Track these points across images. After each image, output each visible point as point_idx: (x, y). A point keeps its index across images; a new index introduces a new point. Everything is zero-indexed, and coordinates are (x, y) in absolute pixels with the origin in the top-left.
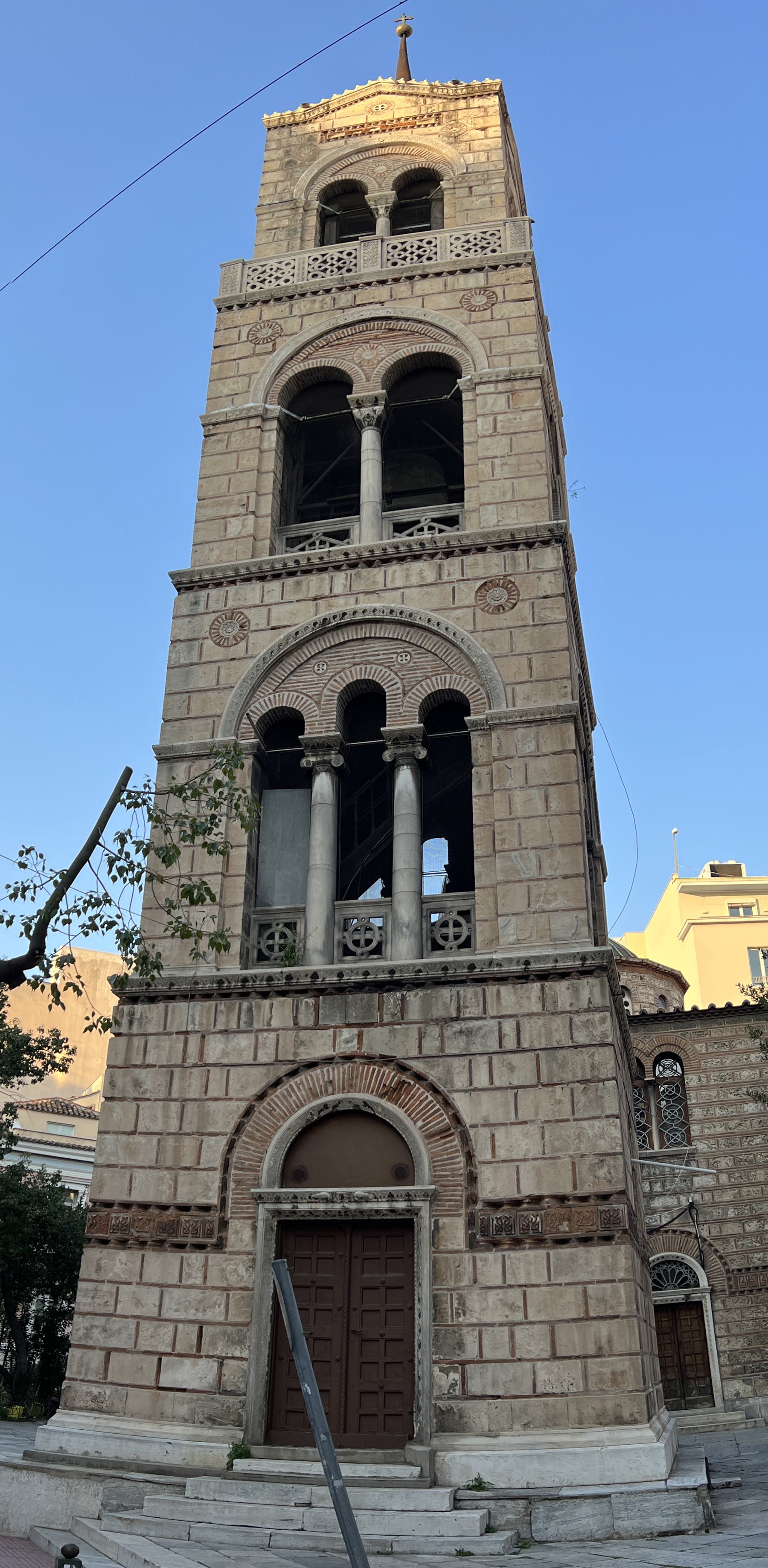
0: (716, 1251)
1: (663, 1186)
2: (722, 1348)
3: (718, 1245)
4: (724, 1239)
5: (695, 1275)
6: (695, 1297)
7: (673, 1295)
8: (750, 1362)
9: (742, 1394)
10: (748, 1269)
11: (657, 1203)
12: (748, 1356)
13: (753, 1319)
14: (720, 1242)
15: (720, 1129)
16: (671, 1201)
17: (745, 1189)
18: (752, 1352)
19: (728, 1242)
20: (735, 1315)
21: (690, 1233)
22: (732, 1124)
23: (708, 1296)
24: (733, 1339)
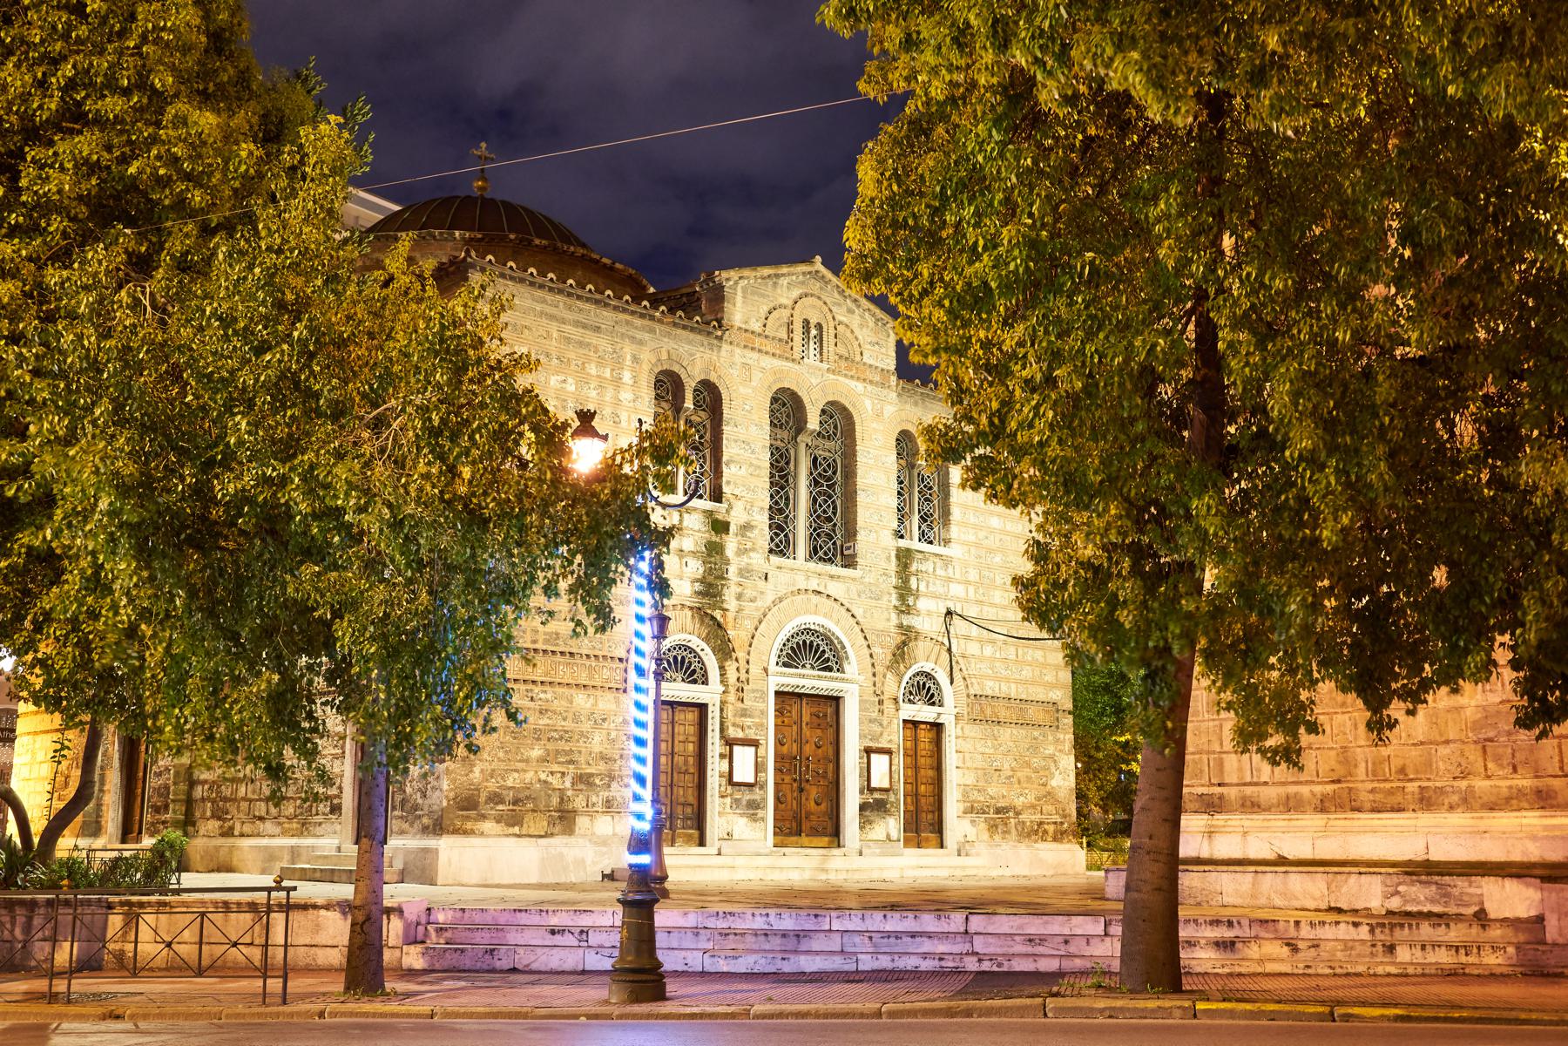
15: (972, 538)
22: (982, 534)
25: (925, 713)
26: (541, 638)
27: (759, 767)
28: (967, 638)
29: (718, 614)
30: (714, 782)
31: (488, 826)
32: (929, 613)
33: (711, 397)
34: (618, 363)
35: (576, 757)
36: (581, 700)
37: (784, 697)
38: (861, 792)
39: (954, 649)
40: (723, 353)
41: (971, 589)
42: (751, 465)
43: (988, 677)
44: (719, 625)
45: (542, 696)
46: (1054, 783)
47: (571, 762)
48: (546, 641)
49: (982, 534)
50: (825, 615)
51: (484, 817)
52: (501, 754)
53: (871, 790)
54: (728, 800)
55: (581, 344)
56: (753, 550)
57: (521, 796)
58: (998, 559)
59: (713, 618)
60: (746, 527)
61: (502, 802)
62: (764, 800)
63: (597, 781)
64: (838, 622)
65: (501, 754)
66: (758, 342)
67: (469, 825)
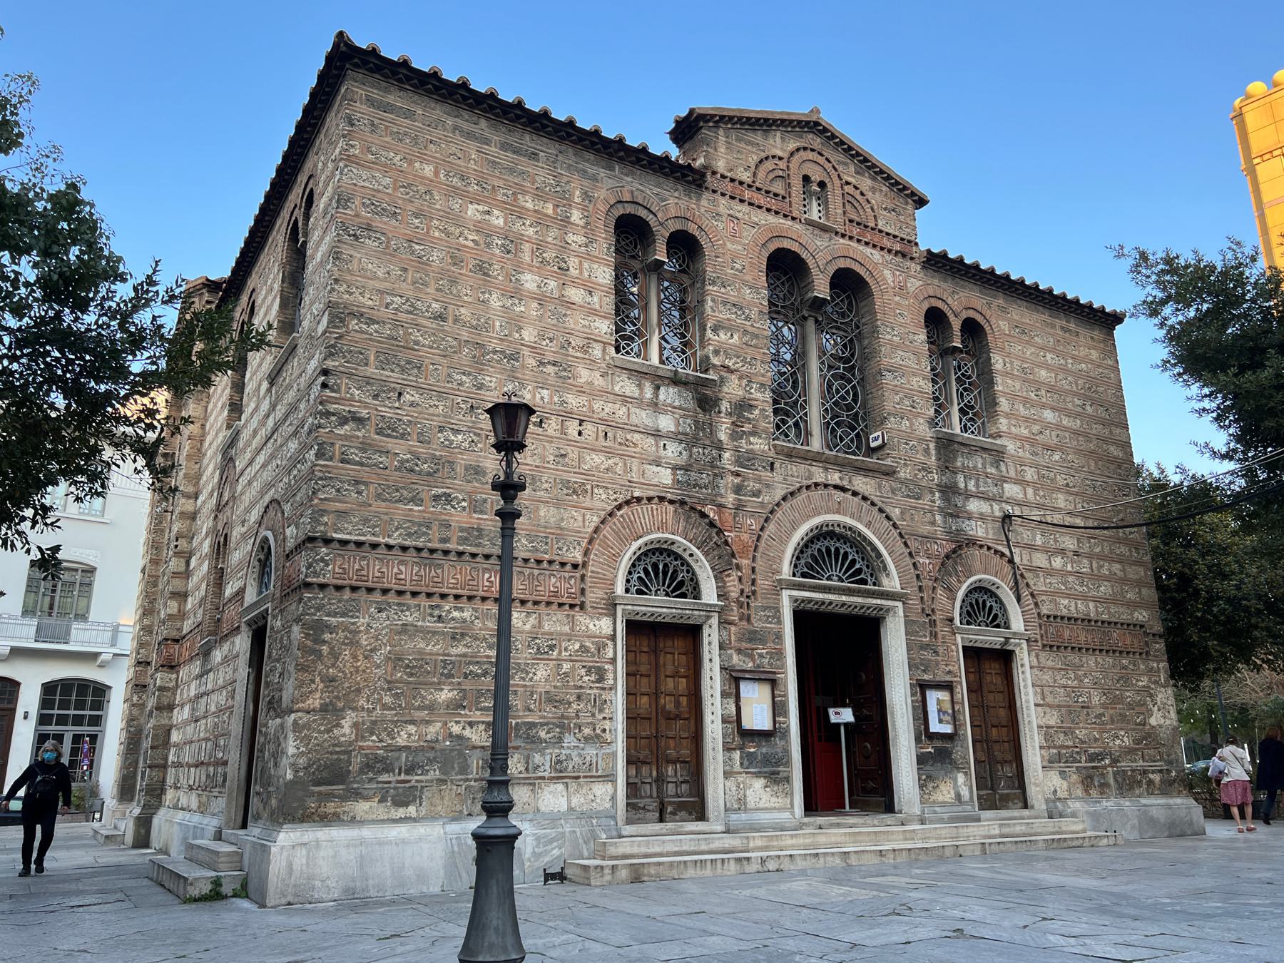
1: (977, 485)
9: (1060, 795)
10: (1055, 617)
12: (1062, 736)
15: (1025, 432)
16: (984, 507)
20: (1047, 677)
21: (1003, 555)
23: (1025, 645)
24: (1048, 710)
25: (989, 638)
26: (455, 535)
27: (778, 709)
28: (1032, 548)
29: (710, 511)
30: (714, 729)
31: (361, 808)
32: (982, 518)
33: (686, 246)
34: (564, 200)
37: (803, 618)
38: (918, 740)
39: (1017, 560)
40: (704, 202)
41: (1030, 491)
42: (746, 332)
44: (712, 524)
45: (456, 614)
46: (1153, 721)
48: (463, 540)
49: (1036, 428)
50: (852, 516)
51: (358, 795)
52: (388, 699)
53: (932, 737)
54: (737, 755)
55: (511, 171)
56: (753, 434)
57: (420, 758)
58: (1056, 457)
59: (704, 515)
60: (743, 406)
61: (388, 769)
62: (787, 751)
63: (543, 734)
64: (868, 525)
65: (388, 699)
66: (747, 194)
67: (331, 807)
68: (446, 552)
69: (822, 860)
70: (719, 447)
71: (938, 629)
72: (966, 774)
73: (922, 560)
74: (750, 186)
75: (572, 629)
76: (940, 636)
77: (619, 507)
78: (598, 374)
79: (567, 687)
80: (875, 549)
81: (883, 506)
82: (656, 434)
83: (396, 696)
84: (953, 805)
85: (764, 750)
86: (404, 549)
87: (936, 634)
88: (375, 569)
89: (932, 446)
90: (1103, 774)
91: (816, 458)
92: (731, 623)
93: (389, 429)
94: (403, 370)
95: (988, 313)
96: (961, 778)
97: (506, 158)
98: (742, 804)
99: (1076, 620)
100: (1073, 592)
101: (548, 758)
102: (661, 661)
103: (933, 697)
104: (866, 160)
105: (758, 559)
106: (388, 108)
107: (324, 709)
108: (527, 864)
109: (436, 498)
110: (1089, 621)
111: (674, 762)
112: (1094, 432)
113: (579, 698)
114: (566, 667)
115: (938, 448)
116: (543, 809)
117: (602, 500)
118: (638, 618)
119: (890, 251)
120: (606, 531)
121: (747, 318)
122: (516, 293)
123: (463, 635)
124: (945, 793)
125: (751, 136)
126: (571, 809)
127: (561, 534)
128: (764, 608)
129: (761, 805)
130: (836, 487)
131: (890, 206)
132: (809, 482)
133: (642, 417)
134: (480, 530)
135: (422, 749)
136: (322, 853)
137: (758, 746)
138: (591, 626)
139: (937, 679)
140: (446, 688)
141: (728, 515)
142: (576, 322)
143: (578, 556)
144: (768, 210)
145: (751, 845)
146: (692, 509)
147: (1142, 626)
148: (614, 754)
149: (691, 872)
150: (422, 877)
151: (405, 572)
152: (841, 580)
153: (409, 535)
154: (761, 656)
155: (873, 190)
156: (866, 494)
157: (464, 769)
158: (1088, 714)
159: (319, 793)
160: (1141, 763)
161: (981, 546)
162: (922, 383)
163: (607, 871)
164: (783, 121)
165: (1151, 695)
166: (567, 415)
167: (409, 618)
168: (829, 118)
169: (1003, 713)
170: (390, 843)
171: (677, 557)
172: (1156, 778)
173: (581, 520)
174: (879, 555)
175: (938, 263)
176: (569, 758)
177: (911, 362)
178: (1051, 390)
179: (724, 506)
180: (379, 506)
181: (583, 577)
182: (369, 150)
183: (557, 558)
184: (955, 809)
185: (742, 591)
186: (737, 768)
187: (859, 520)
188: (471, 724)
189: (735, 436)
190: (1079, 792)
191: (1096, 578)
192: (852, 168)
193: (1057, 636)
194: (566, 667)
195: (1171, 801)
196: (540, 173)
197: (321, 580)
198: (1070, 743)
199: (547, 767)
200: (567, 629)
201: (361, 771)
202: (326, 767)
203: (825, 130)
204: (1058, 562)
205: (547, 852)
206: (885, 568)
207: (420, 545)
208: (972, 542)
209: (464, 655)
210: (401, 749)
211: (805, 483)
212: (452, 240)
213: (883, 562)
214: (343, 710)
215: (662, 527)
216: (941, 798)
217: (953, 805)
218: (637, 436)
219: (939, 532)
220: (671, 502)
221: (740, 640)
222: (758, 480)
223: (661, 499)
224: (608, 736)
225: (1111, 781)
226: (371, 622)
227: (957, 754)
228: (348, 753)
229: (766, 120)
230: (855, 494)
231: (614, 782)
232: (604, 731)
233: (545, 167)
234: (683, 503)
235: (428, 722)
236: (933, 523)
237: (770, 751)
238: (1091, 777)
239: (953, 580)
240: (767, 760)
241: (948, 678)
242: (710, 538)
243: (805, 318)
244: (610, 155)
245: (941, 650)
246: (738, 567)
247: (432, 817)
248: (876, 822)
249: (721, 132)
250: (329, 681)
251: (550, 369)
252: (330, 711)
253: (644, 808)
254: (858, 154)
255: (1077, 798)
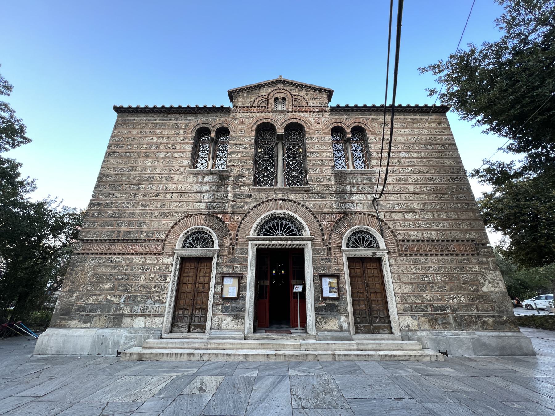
0: (389, 228)
1: (358, 189)
2: (397, 291)
3: (390, 224)
4: (394, 221)
5: (376, 241)
6: (378, 255)
7: (363, 252)
8: (414, 303)
9: (411, 327)
10: (408, 241)
11: (355, 198)
12: (413, 298)
13: (415, 273)
14: (391, 223)
16: (362, 197)
17: (403, 195)
18: (415, 296)
19: (396, 223)
20: (402, 269)
21: (373, 216)
23: (386, 255)
24: (403, 285)
27: (241, 288)
29: (220, 216)
31: (73, 323)
32: (360, 201)
35: (129, 287)
36: (137, 260)
42: (243, 152)
43: (413, 230)
44: (221, 220)
46: (485, 289)
47: (126, 290)
48: (124, 236)
51: (73, 319)
52: (89, 288)
54: (220, 307)
55: (162, 126)
56: (242, 186)
57: (95, 307)
59: (218, 218)
60: (238, 178)
61: (84, 311)
62: (244, 306)
63: (139, 299)
67: (63, 323)
68: (119, 240)
69: (232, 357)
70: (228, 193)
71: (332, 251)
72: (346, 316)
73: (325, 223)
74: (251, 107)
75: (157, 262)
76: (333, 254)
77: (183, 219)
78: (181, 177)
79: (151, 282)
80: (298, 221)
81: (304, 204)
82: (201, 192)
83: (92, 287)
84: (336, 331)
85: (233, 305)
86: (105, 240)
87: (331, 254)
88: (95, 247)
89: (332, 177)
90: (444, 318)
91: (280, 190)
92: (224, 256)
93: (108, 205)
94: (116, 188)
95: (366, 122)
96: (343, 318)
97: (160, 123)
98: (220, 328)
99: (423, 241)
100: (420, 228)
101: (140, 308)
102: (199, 271)
103: (326, 282)
104: (302, 85)
105: (240, 231)
106: (128, 120)
107: (69, 291)
108: (121, 347)
109: (118, 224)
110: (433, 241)
111: (199, 309)
112: (433, 156)
113: (155, 286)
114: (152, 275)
115: (336, 178)
116: (134, 326)
117: (175, 218)
118: (184, 256)
119: (314, 112)
120: (176, 228)
121: (245, 148)
122: (157, 159)
123: (118, 266)
124: (333, 324)
125: (253, 92)
126: (145, 326)
127: (158, 230)
128: (240, 249)
129: (229, 328)
130: (281, 199)
131: (314, 97)
132: (267, 199)
133: (197, 188)
134: (130, 232)
135: (96, 304)
136: (53, 338)
137: (231, 304)
138: (164, 261)
139: (331, 273)
140: (109, 284)
141: (228, 217)
142: (176, 163)
143: (164, 237)
144: (258, 112)
145: (209, 346)
146: (213, 216)
147: (473, 241)
148: (165, 307)
149: (165, 358)
150: (82, 349)
151: (103, 247)
152: (283, 235)
153: (107, 236)
154: (237, 267)
155: (307, 94)
156: (295, 200)
157: (109, 311)
158: (432, 286)
159: (61, 318)
160: (476, 311)
161: (360, 214)
162: (328, 155)
163: (128, 355)
164: (265, 84)
165: (482, 276)
166: (168, 191)
167: (101, 261)
168: (285, 77)
169: (378, 287)
170: (74, 336)
171: (206, 234)
172: (490, 320)
173: (166, 225)
174: (301, 223)
175: (337, 110)
176: (148, 308)
177: (323, 148)
178: (404, 144)
179: (227, 213)
180: (100, 228)
181: (164, 244)
182: (119, 132)
183: (155, 238)
184: (337, 333)
185: (231, 244)
186: (219, 312)
187: (291, 210)
188: (114, 296)
189: (233, 189)
190: (427, 326)
191: (438, 221)
192: (297, 90)
193: (406, 249)
194: (152, 275)
195: (502, 334)
196: (172, 124)
197: (78, 252)
198: (420, 302)
199: (139, 311)
200: (155, 262)
201: (76, 311)
202: (65, 309)
203: (284, 81)
204: (409, 216)
205: (129, 343)
206: (304, 228)
207: (110, 238)
208: (354, 213)
209: (117, 273)
210: (89, 304)
211: (265, 200)
212: (139, 149)
213: (302, 226)
214: (75, 291)
215: (199, 223)
216: (329, 328)
217: (336, 331)
218: (193, 194)
219: (334, 210)
220: (205, 214)
221: (227, 262)
222: (244, 202)
223: (201, 214)
224: (164, 300)
225: (452, 321)
226: (89, 264)
227: (341, 307)
228: (73, 305)
229: (258, 85)
230: (290, 201)
231: (164, 317)
232: (163, 298)
233: (172, 121)
234: (209, 214)
235: (100, 295)
236: (332, 207)
237: (236, 305)
238: (436, 320)
239: (342, 229)
240: (234, 309)
241: (337, 272)
242: (219, 225)
243: (278, 143)
244: (195, 112)
245: (333, 260)
246: (230, 235)
247: (94, 327)
248: (288, 338)
249: (241, 94)
250: (73, 282)
251: (164, 179)
252: (71, 292)
253: (182, 327)
254: (299, 85)
255: (425, 330)
